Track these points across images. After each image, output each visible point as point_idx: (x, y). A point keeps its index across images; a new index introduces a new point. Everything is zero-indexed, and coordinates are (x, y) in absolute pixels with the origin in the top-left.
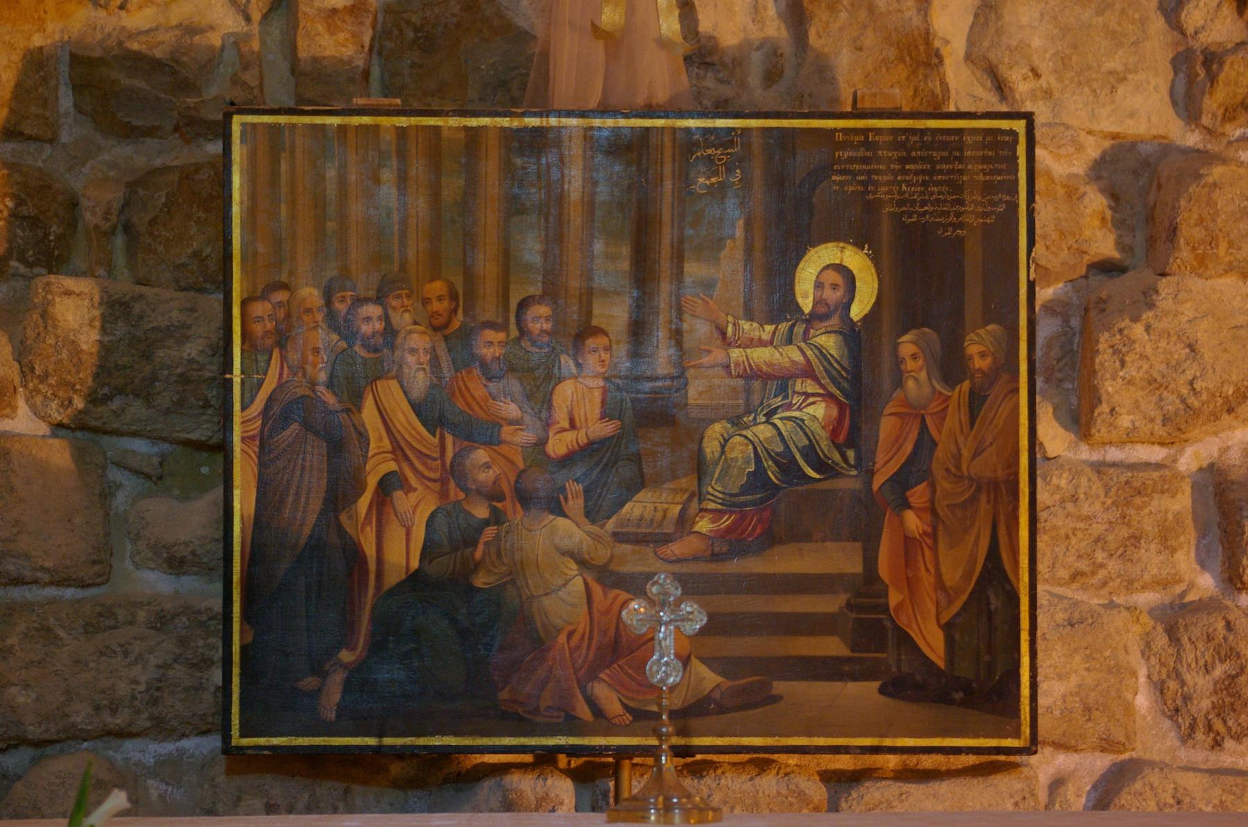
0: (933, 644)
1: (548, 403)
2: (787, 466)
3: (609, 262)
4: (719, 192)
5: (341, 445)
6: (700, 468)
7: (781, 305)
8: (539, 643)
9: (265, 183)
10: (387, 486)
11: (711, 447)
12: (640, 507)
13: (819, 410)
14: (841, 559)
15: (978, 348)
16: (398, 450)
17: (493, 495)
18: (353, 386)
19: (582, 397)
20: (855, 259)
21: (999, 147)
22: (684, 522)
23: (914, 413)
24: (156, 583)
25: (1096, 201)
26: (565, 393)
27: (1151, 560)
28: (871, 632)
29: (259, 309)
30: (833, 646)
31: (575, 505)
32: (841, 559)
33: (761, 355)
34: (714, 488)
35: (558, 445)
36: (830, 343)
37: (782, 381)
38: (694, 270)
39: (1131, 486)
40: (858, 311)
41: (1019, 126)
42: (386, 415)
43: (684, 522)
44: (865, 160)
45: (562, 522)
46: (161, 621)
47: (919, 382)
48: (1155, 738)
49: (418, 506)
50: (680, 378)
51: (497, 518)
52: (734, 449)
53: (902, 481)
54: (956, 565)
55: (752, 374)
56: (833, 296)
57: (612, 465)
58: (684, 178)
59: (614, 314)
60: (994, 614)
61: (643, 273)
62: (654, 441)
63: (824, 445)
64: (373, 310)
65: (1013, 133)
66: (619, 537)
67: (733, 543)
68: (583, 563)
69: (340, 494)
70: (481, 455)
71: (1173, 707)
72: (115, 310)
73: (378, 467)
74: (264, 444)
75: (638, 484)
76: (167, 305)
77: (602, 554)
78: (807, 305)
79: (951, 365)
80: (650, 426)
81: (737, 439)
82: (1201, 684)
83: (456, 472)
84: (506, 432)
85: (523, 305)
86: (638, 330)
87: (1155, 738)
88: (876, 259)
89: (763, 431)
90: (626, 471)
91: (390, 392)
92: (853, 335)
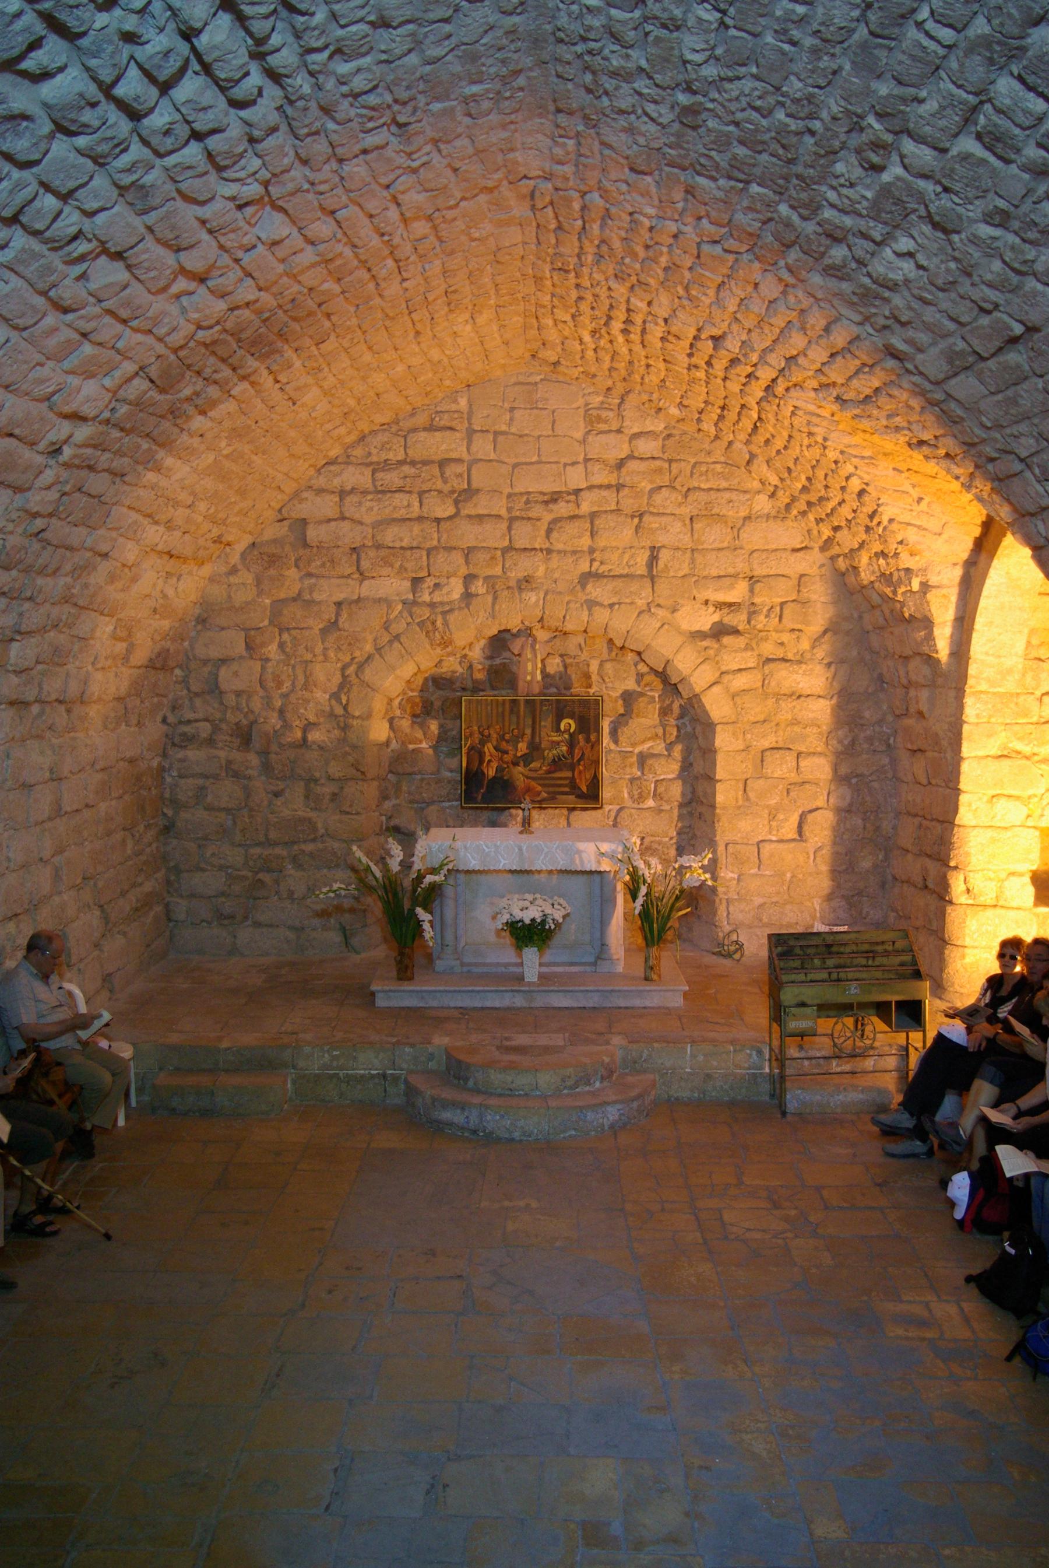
0: (584, 789)
3: (529, 722)
5: (481, 755)
7: (558, 730)
8: (515, 788)
9: (468, 710)
10: (490, 761)
14: (569, 774)
15: (593, 738)
18: (483, 743)
19: (523, 747)
20: (571, 722)
23: (581, 748)
24: (449, 774)
25: (620, 702)
26: (520, 745)
27: (628, 770)
28: (574, 787)
30: (567, 789)
32: (569, 774)
35: (519, 754)
37: (558, 743)
39: (625, 755)
42: (489, 749)
46: (449, 782)
47: (582, 743)
48: (628, 803)
49: (495, 765)
52: (550, 755)
53: (579, 760)
54: (589, 775)
55: (553, 742)
57: (527, 759)
59: (528, 731)
60: (595, 784)
61: (534, 722)
67: (549, 772)
69: (481, 762)
71: (631, 797)
72: (441, 726)
73: (487, 758)
74: (468, 754)
76: (450, 724)
79: (588, 740)
80: (535, 748)
82: (636, 793)
83: (501, 759)
87: (628, 803)
91: (490, 745)
92: (571, 735)
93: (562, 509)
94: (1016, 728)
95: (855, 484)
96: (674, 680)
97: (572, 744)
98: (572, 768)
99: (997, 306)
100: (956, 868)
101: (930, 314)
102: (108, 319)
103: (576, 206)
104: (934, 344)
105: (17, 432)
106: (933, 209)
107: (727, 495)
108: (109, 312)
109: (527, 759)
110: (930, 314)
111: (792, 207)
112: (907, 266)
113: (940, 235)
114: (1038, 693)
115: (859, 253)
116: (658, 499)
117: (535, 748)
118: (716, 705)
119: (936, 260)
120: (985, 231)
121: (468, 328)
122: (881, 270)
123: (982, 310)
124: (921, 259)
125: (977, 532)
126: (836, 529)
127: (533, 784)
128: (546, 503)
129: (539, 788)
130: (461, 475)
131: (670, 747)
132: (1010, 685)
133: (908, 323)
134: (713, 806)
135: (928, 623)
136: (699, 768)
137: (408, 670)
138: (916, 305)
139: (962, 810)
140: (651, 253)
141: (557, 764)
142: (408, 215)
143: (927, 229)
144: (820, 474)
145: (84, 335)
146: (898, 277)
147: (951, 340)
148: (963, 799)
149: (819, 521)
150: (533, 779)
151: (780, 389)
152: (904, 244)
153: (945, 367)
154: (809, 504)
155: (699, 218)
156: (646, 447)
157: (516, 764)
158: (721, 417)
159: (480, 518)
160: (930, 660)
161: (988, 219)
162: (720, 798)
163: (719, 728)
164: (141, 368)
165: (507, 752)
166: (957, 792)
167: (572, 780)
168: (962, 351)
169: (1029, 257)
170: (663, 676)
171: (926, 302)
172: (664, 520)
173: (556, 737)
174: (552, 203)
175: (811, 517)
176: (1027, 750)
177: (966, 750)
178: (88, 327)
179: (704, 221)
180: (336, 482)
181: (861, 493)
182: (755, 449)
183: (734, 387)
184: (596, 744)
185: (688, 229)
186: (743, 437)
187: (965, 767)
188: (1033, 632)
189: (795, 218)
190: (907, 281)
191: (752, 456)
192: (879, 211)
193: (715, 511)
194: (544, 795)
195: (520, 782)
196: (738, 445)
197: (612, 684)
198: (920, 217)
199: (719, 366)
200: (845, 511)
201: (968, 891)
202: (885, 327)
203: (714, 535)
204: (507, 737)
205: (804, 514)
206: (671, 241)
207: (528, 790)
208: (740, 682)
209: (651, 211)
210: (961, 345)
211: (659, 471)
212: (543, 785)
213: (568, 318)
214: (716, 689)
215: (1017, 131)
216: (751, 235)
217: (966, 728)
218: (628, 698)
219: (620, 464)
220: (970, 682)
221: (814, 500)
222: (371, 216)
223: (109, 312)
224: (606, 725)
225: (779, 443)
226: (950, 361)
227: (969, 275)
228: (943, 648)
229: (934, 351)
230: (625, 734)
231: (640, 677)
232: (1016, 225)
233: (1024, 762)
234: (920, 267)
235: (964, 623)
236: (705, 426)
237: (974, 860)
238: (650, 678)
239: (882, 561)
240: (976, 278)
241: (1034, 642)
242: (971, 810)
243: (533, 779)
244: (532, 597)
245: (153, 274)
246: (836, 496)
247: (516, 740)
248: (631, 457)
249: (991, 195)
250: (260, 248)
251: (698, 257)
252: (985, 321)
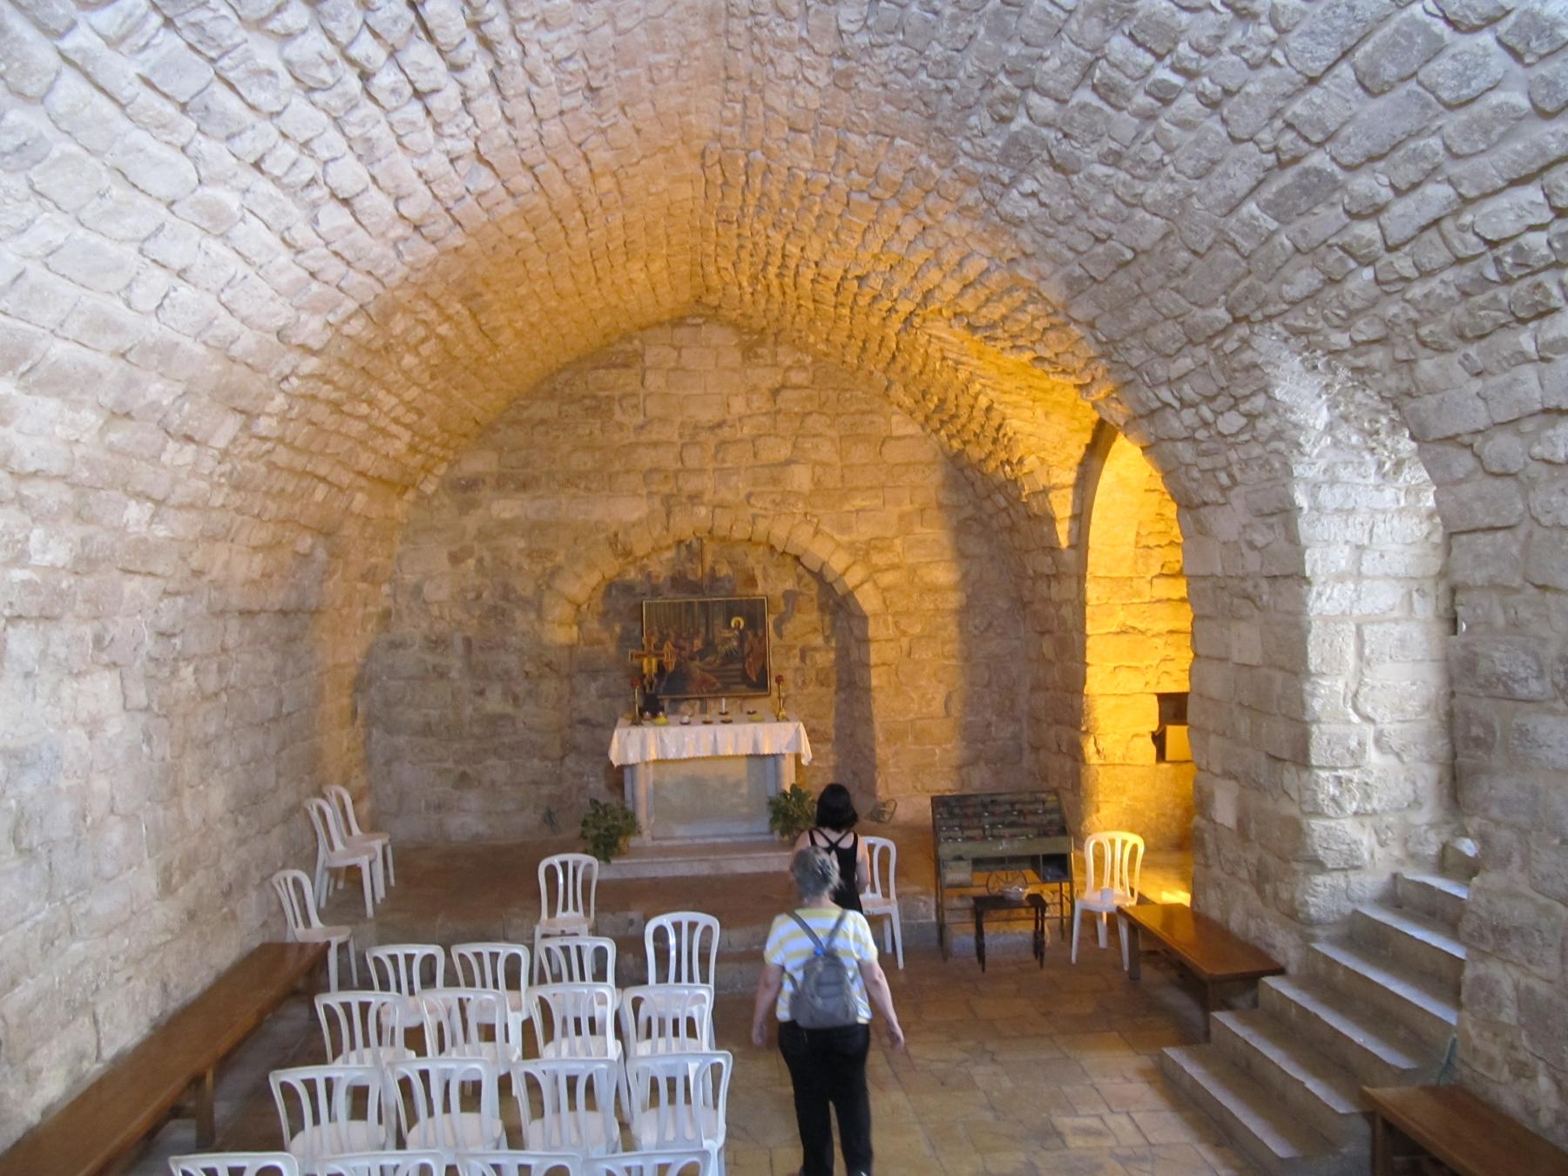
14: (739, 666)
19: (698, 643)
28: (745, 678)
32: (739, 666)
39: (790, 648)
52: (722, 649)
57: (702, 654)
59: (703, 630)
60: (763, 673)
67: (722, 665)
72: (624, 628)
79: (756, 635)
80: (709, 645)
93: (726, 432)
94: (1132, 608)
95: (983, 402)
96: (830, 579)
97: (742, 638)
98: (743, 660)
99: (1110, 236)
100: (1087, 732)
101: (1052, 246)
102: (335, 261)
103: (742, 163)
104: (1055, 272)
105: (250, 361)
106: (1054, 153)
107: (869, 417)
108: (336, 254)
109: (702, 654)
110: (1052, 246)
111: (931, 157)
112: (1032, 205)
113: (1060, 176)
114: (1149, 577)
115: (989, 195)
116: (810, 421)
117: (709, 645)
118: (868, 600)
119: (1057, 198)
120: (1100, 170)
121: (643, 276)
122: (1009, 209)
123: (1097, 240)
124: (1043, 197)
125: (1087, 438)
126: (965, 443)
127: (708, 676)
128: (712, 428)
130: (635, 406)
131: (827, 639)
132: (1124, 571)
133: (1033, 254)
134: (868, 690)
135: (1051, 520)
136: (854, 655)
137: (594, 578)
138: (1039, 238)
139: (1089, 681)
140: (806, 202)
141: (729, 657)
142: (597, 170)
143: (1049, 171)
144: (951, 396)
145: (312, 274)
146: (1025, 214)
147: (1069, 268)
148: (1089, 671)
149: (950, 437)
151: (917, 321)
152: (1029, 185)
153: (1065, 292)
154: (942, 422)
155: (849, 170)
156: (797, 377)
157: (692, 658)
158: (864, 349)
159: (655, 445)
160: (1053, 549)
161: (1103, 159)
162: (874, 682)
163: (871, 621)
164: (361, 306)
166: (1085, 664)
167: (744, 671)
168: (1080, 278)
169: (1139, 191)
170: (819, 576)
171: (1048, 236)
172: (815, 440)
173: (729, 632)
174: (720, 161)
175: (943, 433)
176: (1142, 626)
177: (1089, 629)
178: (314, 266)
179: (854, 173)
180: (525, 414)
181: (989, 409)
182: (893, 376)
183: (875, 321)
184: (762, 639)
185: (839, 180)
186: (881, 366)
187: (1089, 643)
188: (1140, 523)
189: (933, 166)
190: (1031, 218)
191: (891, 383)
192: (1007, 157)
193: (860, 431)
195: (697, 673)
196: (878, 374)
197: (773, 585)
198: (1043, 161)
199: (863, 301)
200: (975, 427)
201: (1098, 752)
202: (1012, 260)
203: (859, 454)
205: (937, 431)
206: (824, 191)
208: (888, 579)
209: (807, 165)
210: (1078, 271)
211: (810, 398)
213: (730, 266)
214: (867, 586)
215: (1128, 82)
216: (895, 183)
217: (1088, 610)
218: (789, 596)
219: (775, 393)
220: (1090, 569)
221: (945, 418)
222: (565, 171)
223: (336, 254)
224: (770, 620)
225: (915, 369)
226: (1069, 285)
227: (1086, 209)
228: (1064, 541)
229: (1057, 277)
230: (788, 628)
231: (800, 578)
232: (1127, 163)
233: (1140, 637)
234: (1042, 204)
235: (1081, 517)
236: (848, 359)
237: (1101, 724)
238: (808, 578)
239: (1007, 468)
240: (1092, 211)
241: (1143, 532)
242: (1096, 682)
244: (703, 511)
245: (373, 219)
246: (964, 412)
247: (690, 638)
248: (783, 387)
249: (1106, 138)
250: (469, 199)
251: (848, 204)
252: (1100, 249)
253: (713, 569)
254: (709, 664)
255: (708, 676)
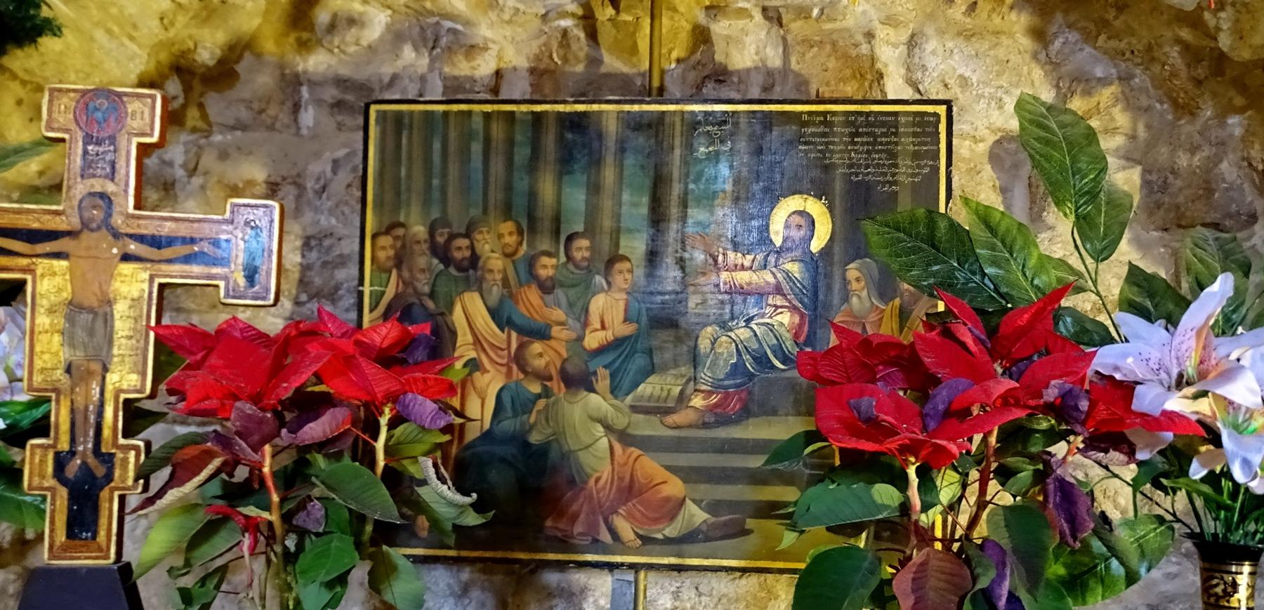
1: (586, 311)
2: (761, 360)
3: (635, 207)
4: (715, 157)
6: (695, 359)
8: (576, 481)
11: (704, 345)
12: (647, 388)
13: (785, 318)
16: (477, 342)
17: (543, 377)
19: (609, 311)
20: (816, 208)
21: (925, 126)
22: (682, 399)
26: (598, 304)
29: (385, 241)
31: (603, 383)
33: (743, 277)
34: (705, 375)
35: (593, 340)
36: (795, 269)
38: (696, 214)
40: (816, 245)
41: (942, 110)
43: (682, 399)
44: (824, 135)
45: (593, 395)
49: (491, 383)
50: (681, 295)
51: (547, 393)
52: (721, 347)
56: (797, 234)
57: (628, 358)
58: (689, 147)
59: (635, 246)
61: (657, 218)
62: (663, 337)
63: (789, 345)
64: (464, 242)
65: (936, 115)
66: (635, 409)
67: (718, 416)
68: (608, 428)
70: (537, 347)
75: (651, 370)
77: (620, 422)
78: (778, 241)
80: (662, 328)
81: (724, 338)
83: (519, 359)
84: (555, 331)
85: (570, 239)
86: (653, 257)
88: (831, 209)
89: (743, 333)
90: (639, 361)
109: (628, 358)
117: (662, 328)
127: (650, 467)
129: (674, 487)
150: (647, 444)
157: (578, 381)
165: (542, 334)
194: (696, 515)
195: (597, 457)
204: (547, 267)
207: (630, 490)
212: (689, 475)
243: (647, 444)
247: (576, 287)
253: (701, 37)
254: (659, 410)
255: (650, 467)
